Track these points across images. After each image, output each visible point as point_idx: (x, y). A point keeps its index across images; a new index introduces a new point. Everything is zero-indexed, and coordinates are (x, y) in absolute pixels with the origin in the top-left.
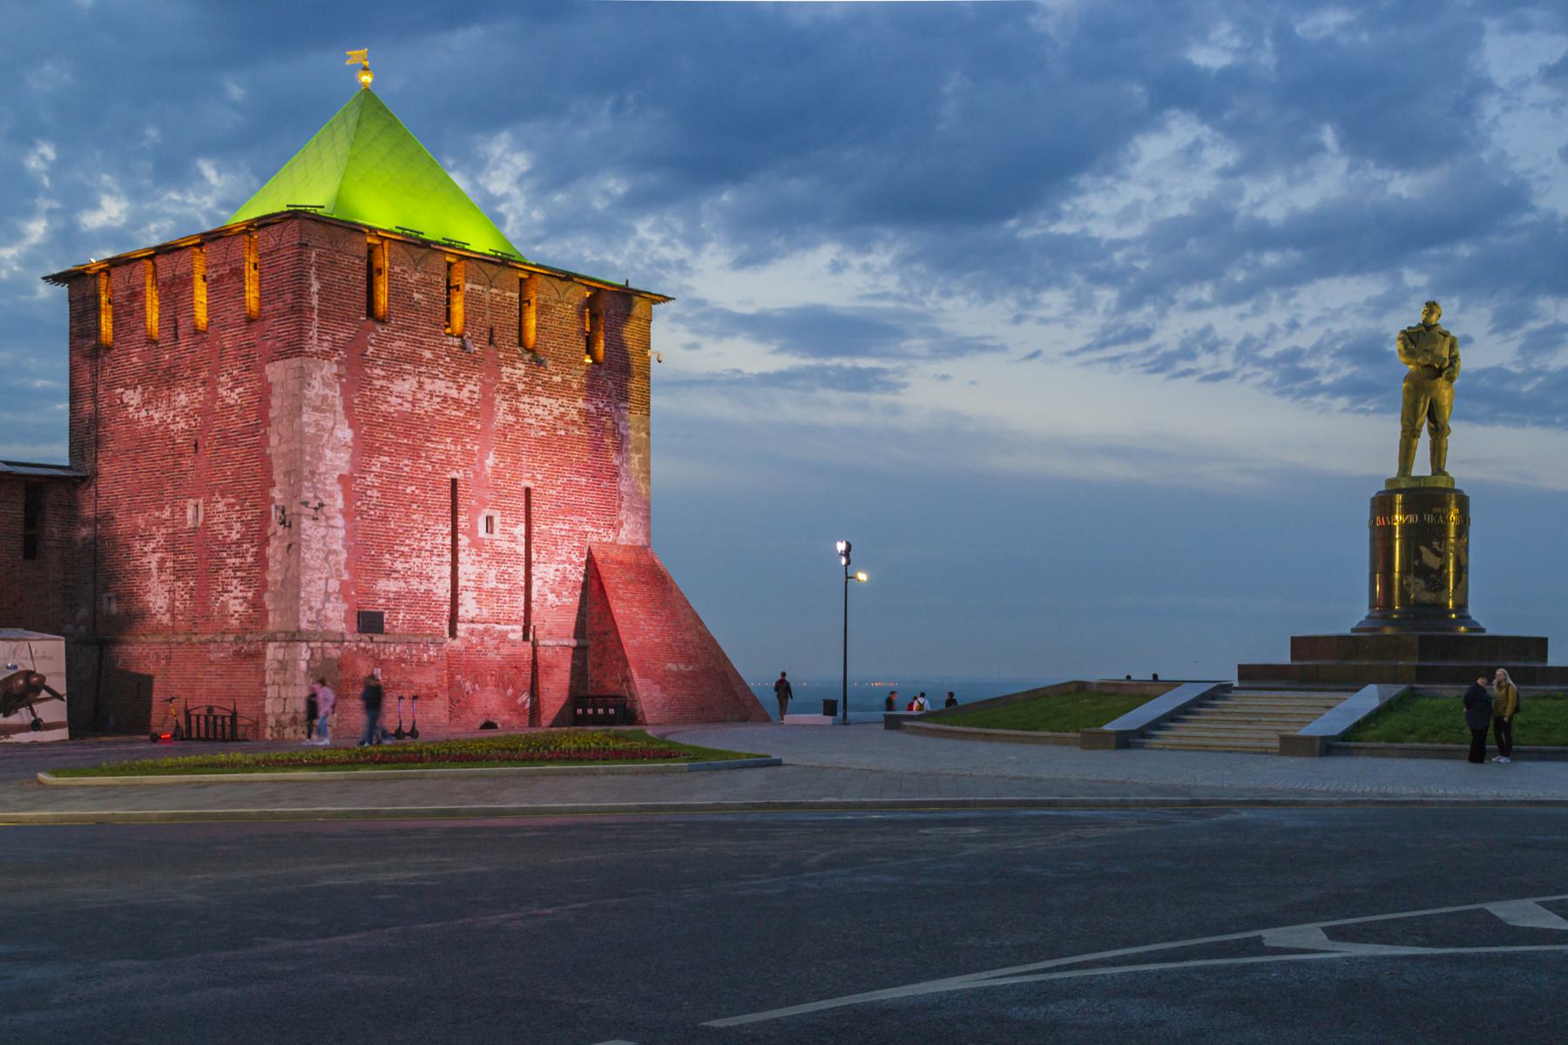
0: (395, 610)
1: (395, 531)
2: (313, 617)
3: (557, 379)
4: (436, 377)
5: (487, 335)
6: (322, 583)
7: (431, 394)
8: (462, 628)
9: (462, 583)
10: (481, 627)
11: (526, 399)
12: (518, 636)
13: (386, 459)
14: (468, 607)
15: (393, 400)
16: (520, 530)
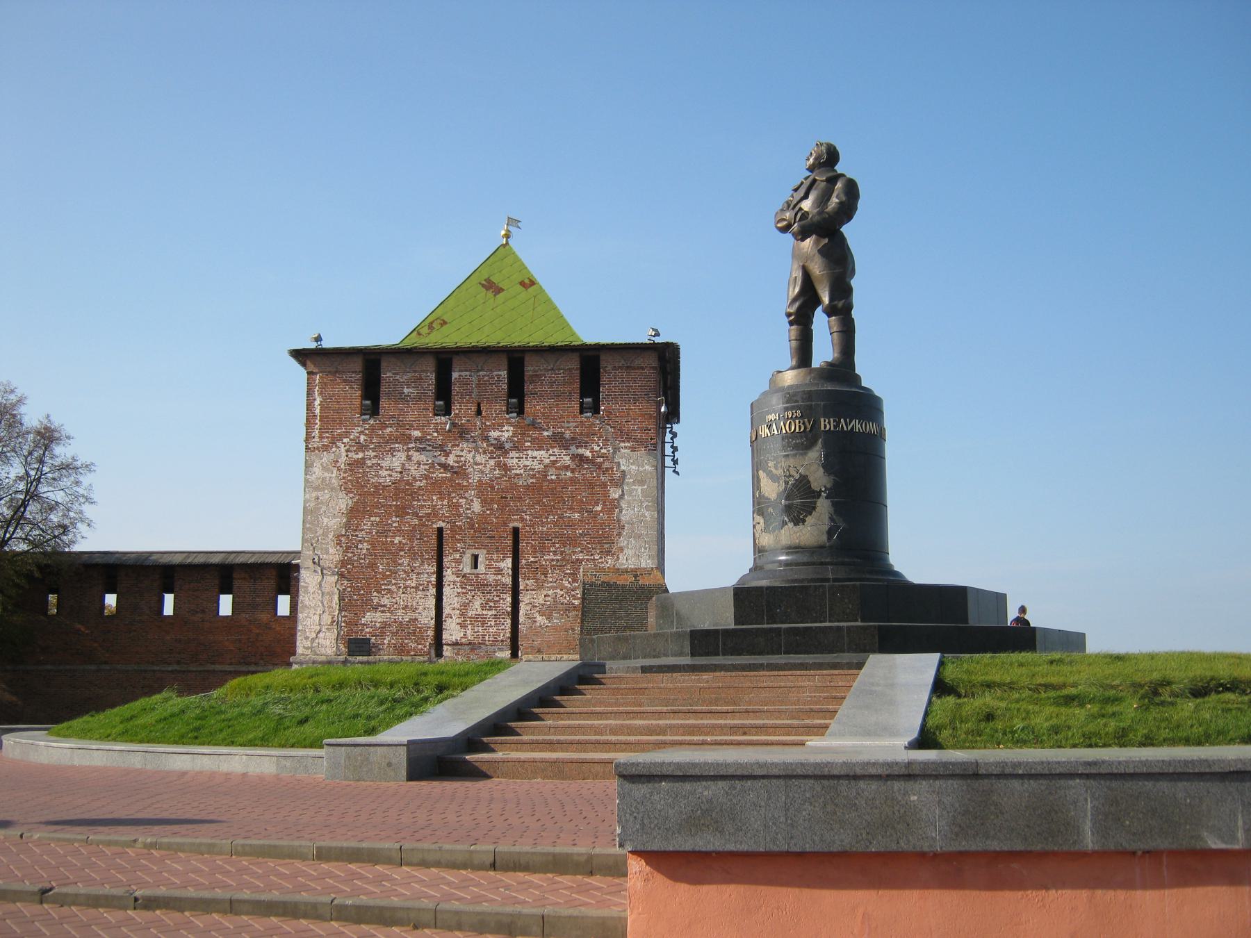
1: (384, 574)
2: (308, 644)
6: (317, 617)
7: (419, 463)
8: (447, 651)
9: (446, 611)
11: (514, 454)
12: (507, 654)
14: (452, 632)
15: (383, 473)
16: (508, 563)
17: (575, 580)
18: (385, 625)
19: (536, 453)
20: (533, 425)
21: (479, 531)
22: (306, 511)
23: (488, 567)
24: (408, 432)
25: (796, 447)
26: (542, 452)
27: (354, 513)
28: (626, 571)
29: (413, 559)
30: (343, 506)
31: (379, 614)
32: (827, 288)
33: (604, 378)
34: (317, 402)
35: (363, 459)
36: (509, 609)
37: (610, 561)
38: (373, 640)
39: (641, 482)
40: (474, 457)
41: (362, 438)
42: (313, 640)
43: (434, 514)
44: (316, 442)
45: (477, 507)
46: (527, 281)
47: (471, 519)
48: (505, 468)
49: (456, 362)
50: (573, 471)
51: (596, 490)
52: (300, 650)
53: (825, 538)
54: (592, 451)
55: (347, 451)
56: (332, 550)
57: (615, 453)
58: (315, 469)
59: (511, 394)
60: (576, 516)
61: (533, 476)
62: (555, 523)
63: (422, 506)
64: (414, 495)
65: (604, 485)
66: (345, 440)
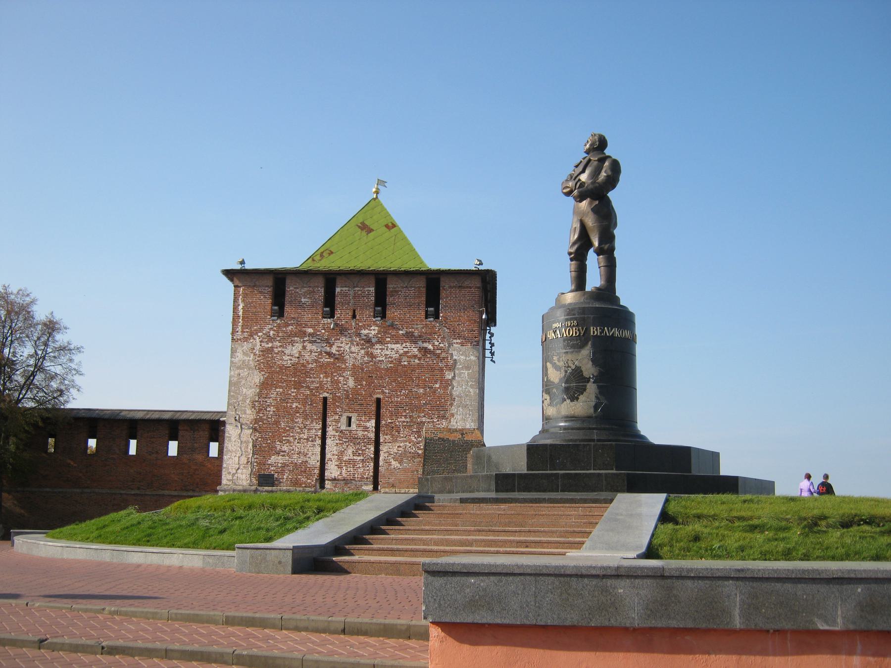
0: (282, 472)
1: (285, 429)
2: (230, 477)
6: (237, 459)
7: (311, 351)
8: (328, 485)
9: (328, 456)
11: (378, 346)
12: (370, 487)
14: (332, 470)
16: (372, 423)
17: (419, 436)
18: (284, 465)
19: (393, 346)
20: (392, 326)
21: (353, 400)
22: (231, 383)
23: (359, 426)
24: (304, 329)
25: (573, 346)
26: (398, 345)
27: (265, 386)
28: (456, 430)
29: (306, 418)
30: (257, 381)
31: (280, 457)
32: (597, 236)
33: (443, 294)
34: (241, 307)
35: (272, 347)
36: (372, 456)
37: (444, 424)
38: (276, 476)
40: (350, 348)
41: (272, 332)
42: (234, 474)
43: (321, 387)
44: (239, 335)
45: (351, 383)
46: (390, 224)
47: (347, 391)
48: (372, 356)
49: (339, 281)
50: (419, 359)
51: (437, 373)
52: (224, 482)
53: (592, 410)
54: (433, 345)
55: (261, 342)
56: (249, 412)
57: (449, 346)
58: (238, 354)
59: (377, 304)
60: (421, 390)
62: (406, 396)
63: (313, 382)
64: (307, 374)
65: (441, 370)
66: (260, 334)
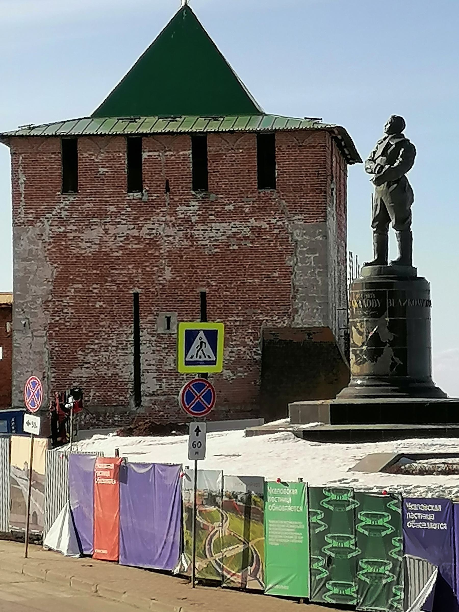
1: (86, 334)
3: (227, 208)
4: (119, 223)
5: (163, 186)
8: (145, 401)
9: (143, 367)
10: (162, 398)
11: (200, 227)
13: (80, 286)
14: (149, 384)
15: (83, 245)
18: (90, 380)
21: (172, 297)
25: (373, 316)
34: (21, 181)
39: (311, 251)
40: (164, 229)
45: (168, 274)
61: (217, 247)
65: (281, 255)
66: (48, 215)
